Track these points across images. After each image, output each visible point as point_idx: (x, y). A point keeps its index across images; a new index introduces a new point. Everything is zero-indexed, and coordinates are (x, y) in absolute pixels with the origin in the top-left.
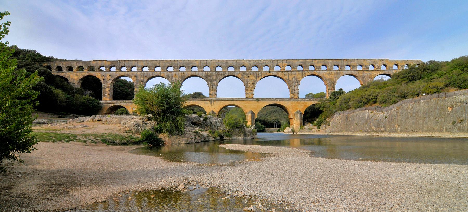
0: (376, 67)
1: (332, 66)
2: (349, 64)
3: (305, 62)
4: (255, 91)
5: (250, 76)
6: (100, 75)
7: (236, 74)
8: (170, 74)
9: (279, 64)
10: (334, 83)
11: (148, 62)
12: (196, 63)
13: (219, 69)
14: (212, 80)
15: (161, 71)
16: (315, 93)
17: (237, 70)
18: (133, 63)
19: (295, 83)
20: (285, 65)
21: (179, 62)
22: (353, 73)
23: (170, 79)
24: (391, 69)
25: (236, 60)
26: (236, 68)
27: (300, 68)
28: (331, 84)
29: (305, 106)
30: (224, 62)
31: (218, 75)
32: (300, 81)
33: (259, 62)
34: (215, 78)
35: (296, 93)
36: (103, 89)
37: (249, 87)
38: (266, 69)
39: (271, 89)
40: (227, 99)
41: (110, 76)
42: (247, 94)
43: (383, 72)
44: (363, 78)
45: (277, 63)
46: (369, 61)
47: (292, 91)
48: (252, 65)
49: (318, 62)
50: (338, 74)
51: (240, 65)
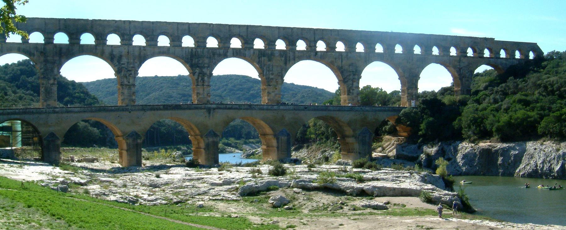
1: (413, 47)
13: (212, 42)
17: (248, 46)
19: (354, 75)
23: (115, 61)
24: (497, 56)
25: (248, 26)
28: (410, 78)
31: (214, 54)
34: (206, 61)
35: (355, 95)
44: (460, 69)
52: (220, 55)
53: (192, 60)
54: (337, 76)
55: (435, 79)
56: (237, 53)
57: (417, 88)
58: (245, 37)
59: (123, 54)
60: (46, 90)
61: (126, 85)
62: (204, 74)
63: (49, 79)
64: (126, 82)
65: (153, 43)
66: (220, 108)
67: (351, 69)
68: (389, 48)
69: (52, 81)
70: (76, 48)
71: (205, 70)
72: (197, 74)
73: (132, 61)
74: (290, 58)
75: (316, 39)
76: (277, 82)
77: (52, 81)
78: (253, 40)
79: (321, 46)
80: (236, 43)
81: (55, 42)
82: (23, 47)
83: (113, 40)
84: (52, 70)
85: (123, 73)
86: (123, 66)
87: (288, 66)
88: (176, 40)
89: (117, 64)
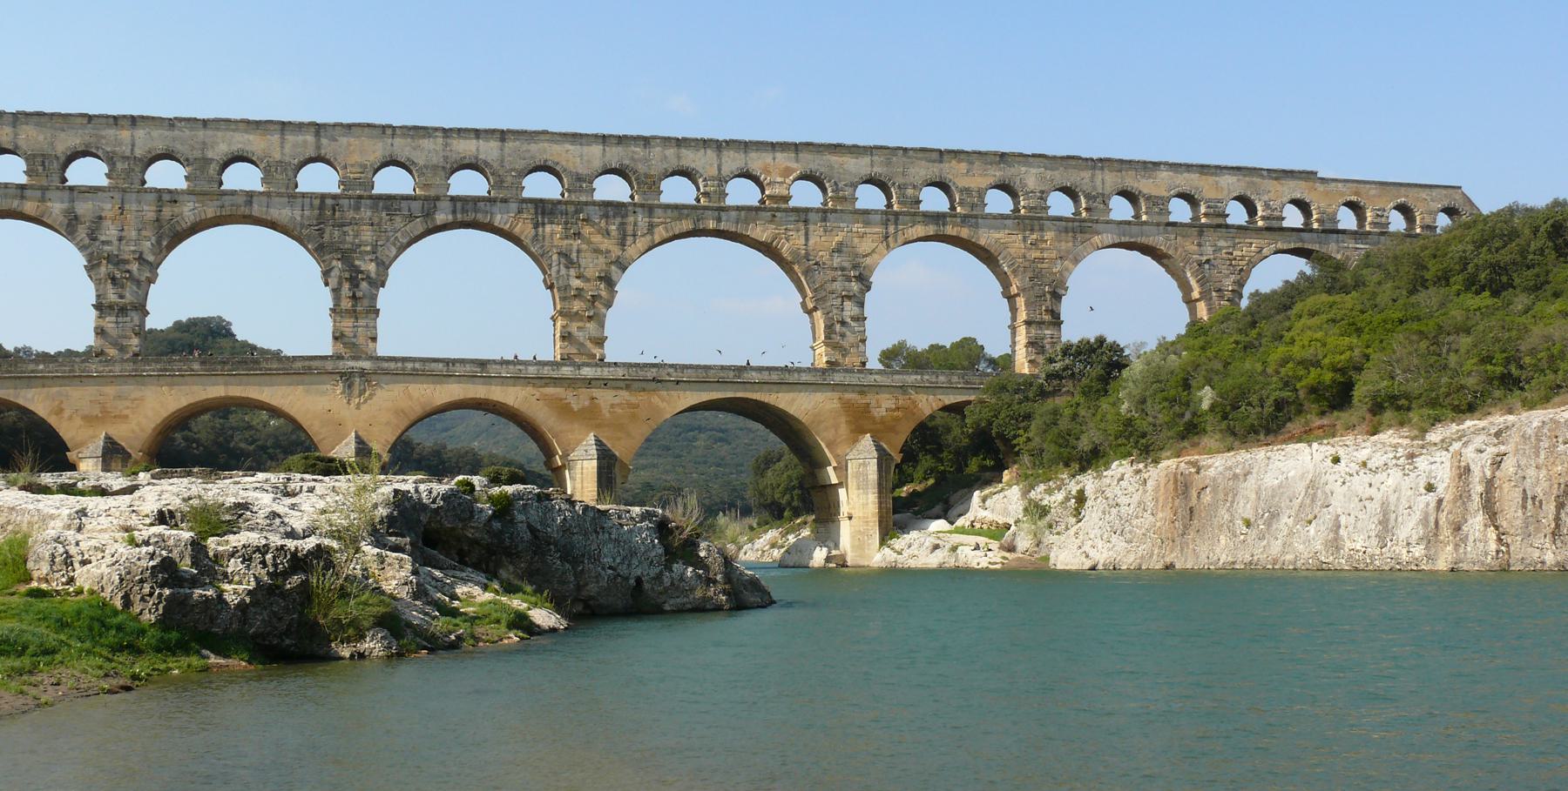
1: (1043, 196)
4: (614, 319)
8: (84, 208)
12: (254, 143)
13: (393, 182)
14: (351, 245)
15: (23, 180)
16: (920, 343)
20: (786, 172)
21: (140, 133)
23: (82, 232)
26: (497, 182)
27: (868, 197)
32: (871, 269)
33: (639, 150)
34: (367, 235)
37: (583, 302)
38: (677, 191)
39: (705, 309)
40: (445, 369)
42: (566, 337)
46: (1227, 180)
47: (829, 328)
48: (597, 164)
51: (521, 164)
53: (321, 232)
56: (469, 215)
57: (1056, 322)
58: (495, 165)
59: (107, 214)
61: (111, 307)
64: (112, 296)
66: (387, 373)
67: (837, 261)
72: (335, 273)
73: (134, 234)
75: (726, 171)
80: (469, 184)
83: (88, 173)
85: (103, 269)
86: (107, 248)
87: (631, 251)
88: (281, 173)
89: (87, 241)
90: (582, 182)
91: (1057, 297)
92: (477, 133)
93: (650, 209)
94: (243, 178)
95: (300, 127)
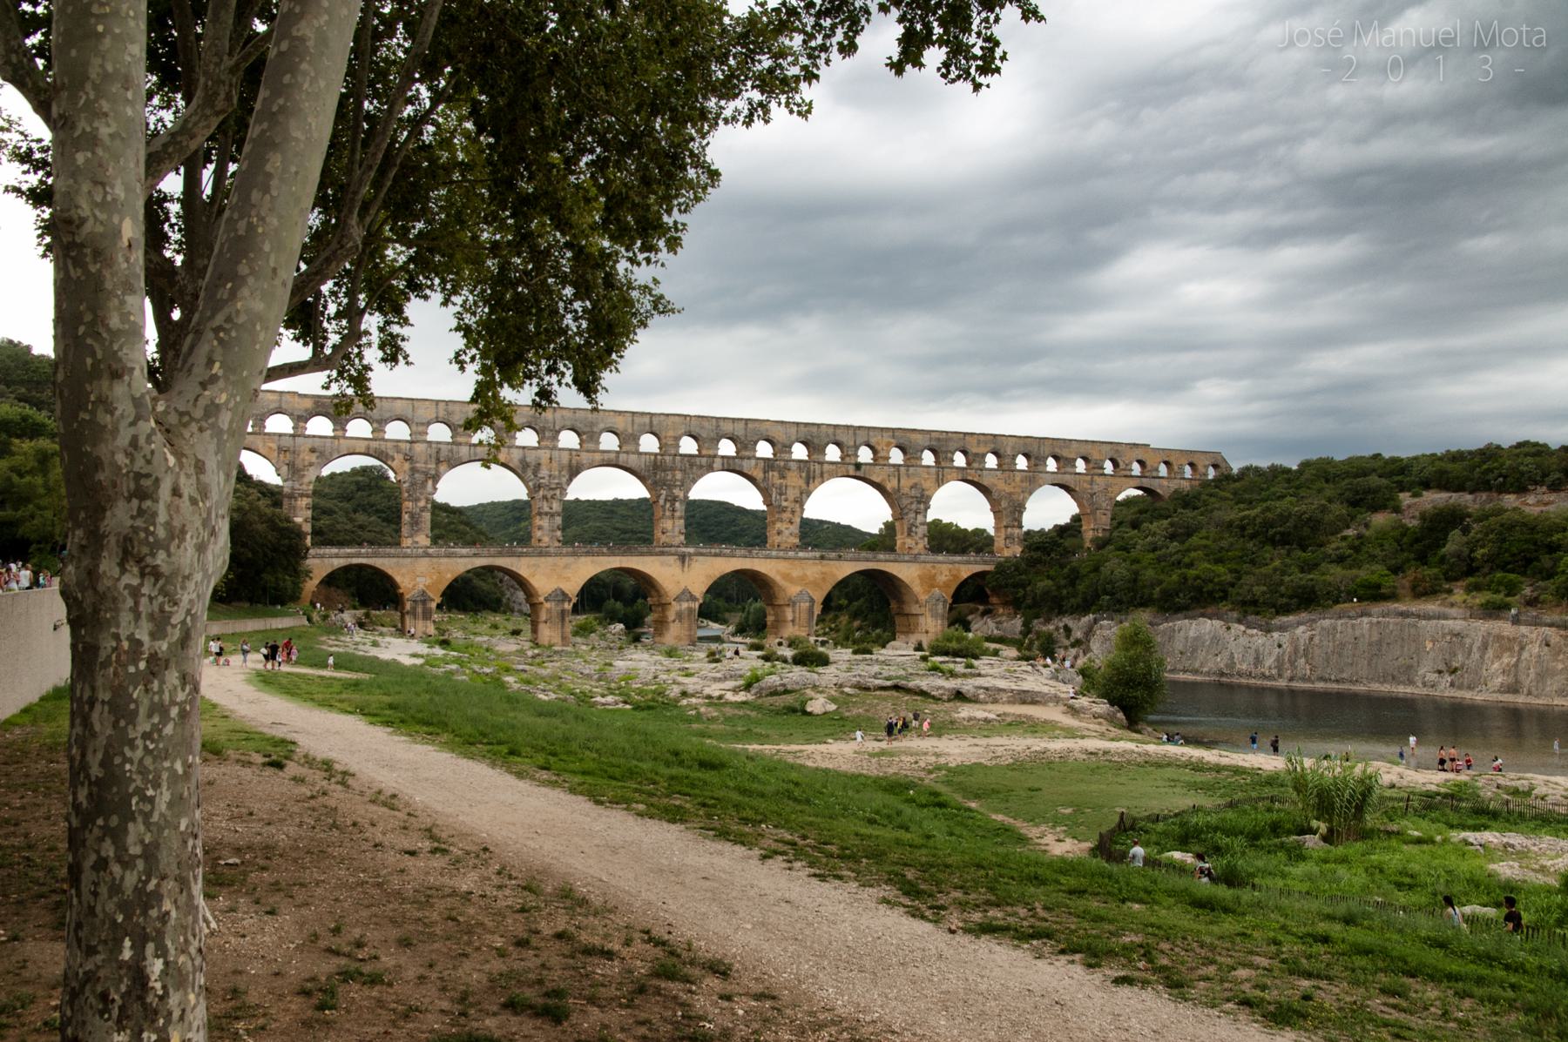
0: (1122, 466)
1: (1014, 457)
2: (1058, 451)
3: (947, 440)
5: (789, 474)
6: (274, 446)
7: (747, 466)
9: (873, 441)
10: (1019, 509)
11: (451, 407)
12: (620, 423)
13: (688, 446)
17: (747, 454)
18: (399, 407)
22: (1067, 479)
23: (530, 473)
27: (928, 458)
28: (1008, 508)
29: (956, 577)
30: (706, 424)
31: (692, 465)
32: (929, 498)
33: (815, 429)
34: (679, 475)
36: (286, 502)
41: (313, 450)
43: (1137, 482)
45: (867, 435)
47: (910, 530)
49: (979, 442)
50: (1033, 480)
52: (701, 467)
54: (892, 506)
55: (1048, 509)
56: (730, 466)
60: (412, 516)
62: (675, 499)
63: (417, 500)
64: (546, 509)
65: (591, 446)
66: (702, 554)
67: (913, 492)
68: (974, 459)
69: (422, 504)
70: (464, 450)
71: (676, 491)
74: (814, 473)
76: (793, 512)
77: (422, 504)
78: (756, 443)
79: (865, 455)
80: (727, 448)
81: (429, 438)
82: (374, 445)
84: (424, 484)
88: (628, 439)
90: (788, 448)
91: (1021, 513)
92: (734, 420)
93: (821, 463)
94: (609, 442)
95: (643, 414)
